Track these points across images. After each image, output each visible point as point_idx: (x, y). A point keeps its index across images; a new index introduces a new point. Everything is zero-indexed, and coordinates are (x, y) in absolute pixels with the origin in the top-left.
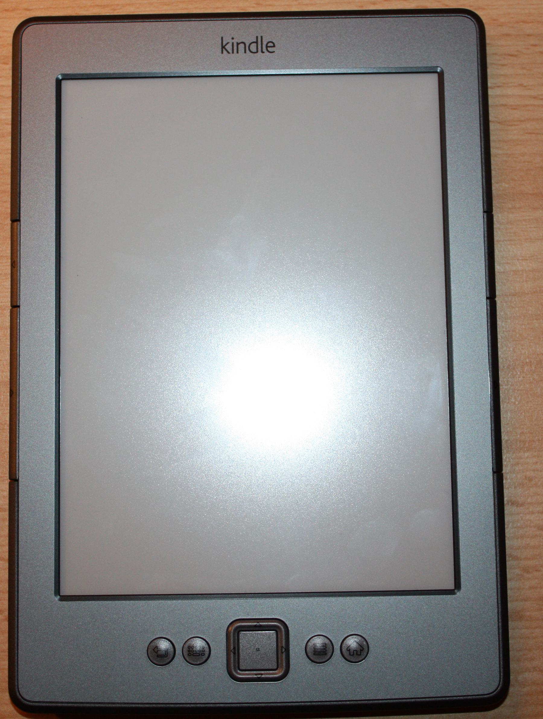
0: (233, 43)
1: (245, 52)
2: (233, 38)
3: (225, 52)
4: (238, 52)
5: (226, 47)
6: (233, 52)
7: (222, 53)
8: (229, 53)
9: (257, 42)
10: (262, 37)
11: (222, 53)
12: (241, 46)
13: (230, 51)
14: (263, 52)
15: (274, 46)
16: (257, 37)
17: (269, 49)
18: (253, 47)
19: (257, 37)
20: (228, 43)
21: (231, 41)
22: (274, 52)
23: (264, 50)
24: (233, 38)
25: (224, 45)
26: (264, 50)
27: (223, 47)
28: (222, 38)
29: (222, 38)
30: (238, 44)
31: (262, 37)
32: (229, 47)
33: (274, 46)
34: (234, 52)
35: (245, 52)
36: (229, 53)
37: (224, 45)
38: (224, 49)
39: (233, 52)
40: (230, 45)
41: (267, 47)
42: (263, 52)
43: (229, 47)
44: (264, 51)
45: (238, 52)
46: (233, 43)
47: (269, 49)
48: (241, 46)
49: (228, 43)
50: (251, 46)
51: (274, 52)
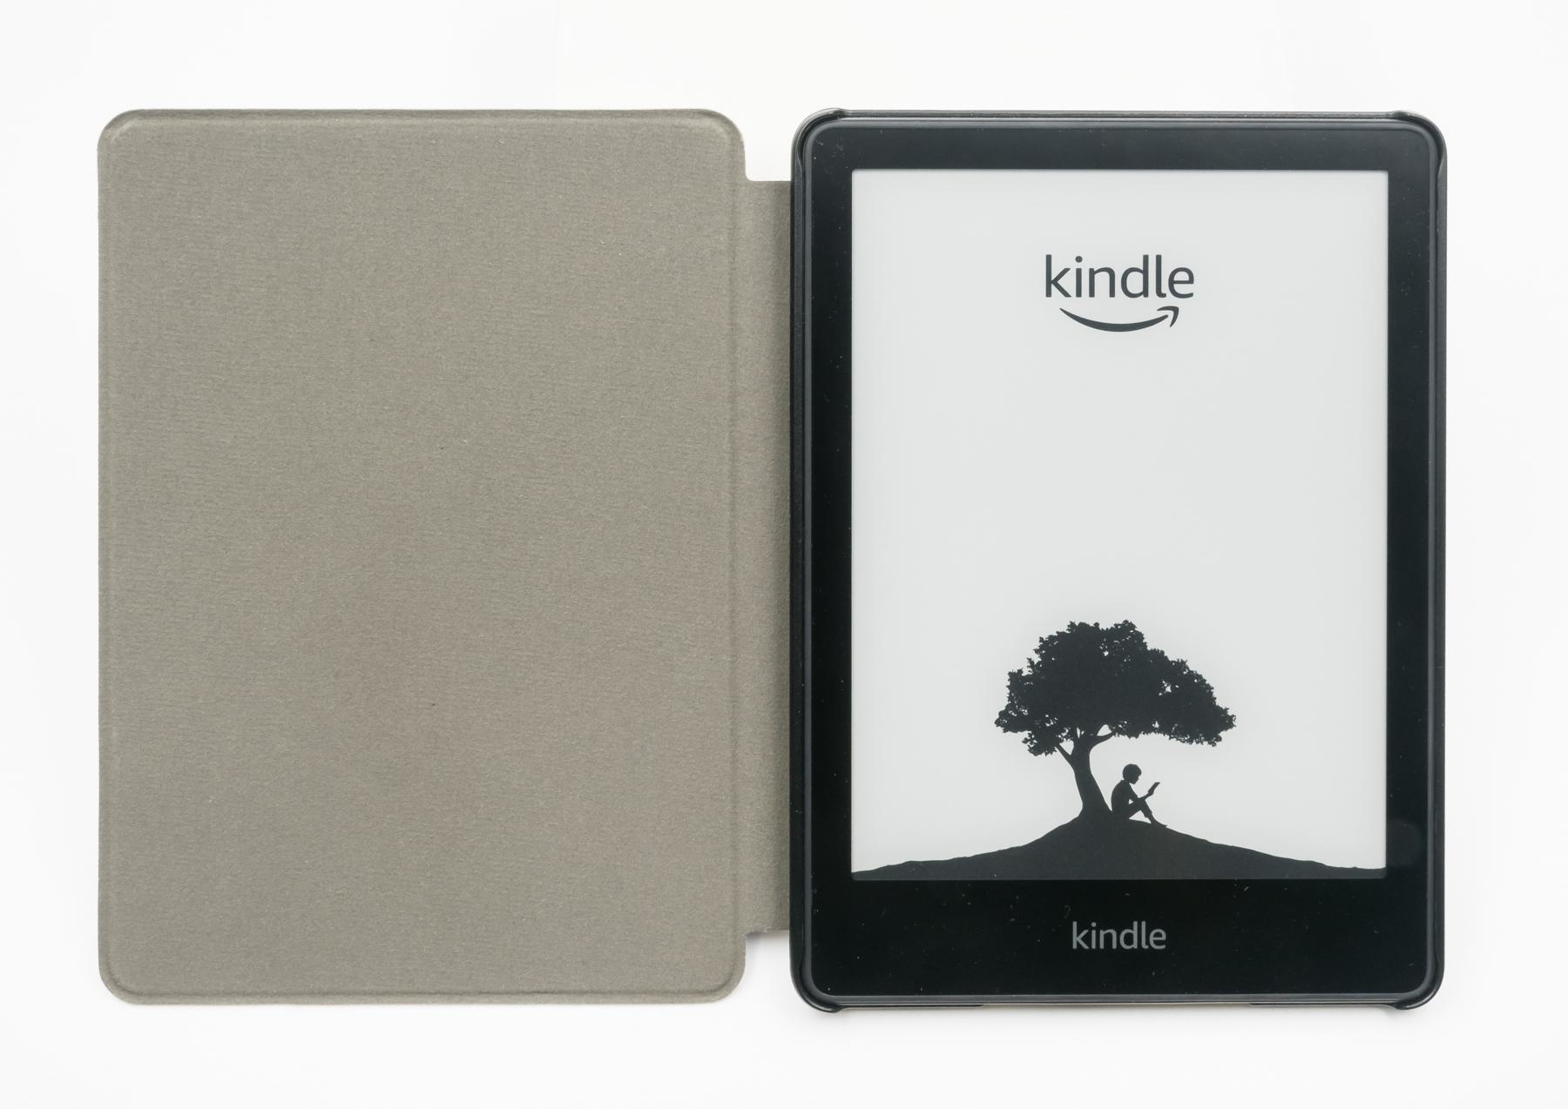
0: (1079, 272)
1: (1112, 294)
2: (1079, 259)
4: (1092, 294)
5: (1060, 282)
6: (1079, 294)
7: (1049, 294)
8: (1066, 295)
9: (1145, 272)
10: (1159, 258)
11: (1049, 294)
12: (1102, 280)
13: (1072, 290)
14: (1160, 294)
15: (1191, 281)
16: (1146, 258)
18: (1135, 283)
19: (1146, 258)
20: (1066, 271)
21: (1074, 266)
23: (1165, 288)
26: (1165, 288)
27: (1052, 283)
28: (1049, 258)
29: (1049, 258)
30: (1092, 273)
31: (1159, 258)
32: (1068, 282)
33: (1191, 281)
34: (1083, 294)
35: (1112, 294)
36: (1066, 295)
37: (1053, 277)
38: (1053, 286)
39: (1079, 294)
40: (1071, 276)
41: (1172, 282)
43: (1068, 282)
44: (1163, 291)
45: (1092, 294)
46: (1079, 272)
47: (1178, 288)
48: (1102, 280)
49: (1066, 271)
50: (1131, 276)
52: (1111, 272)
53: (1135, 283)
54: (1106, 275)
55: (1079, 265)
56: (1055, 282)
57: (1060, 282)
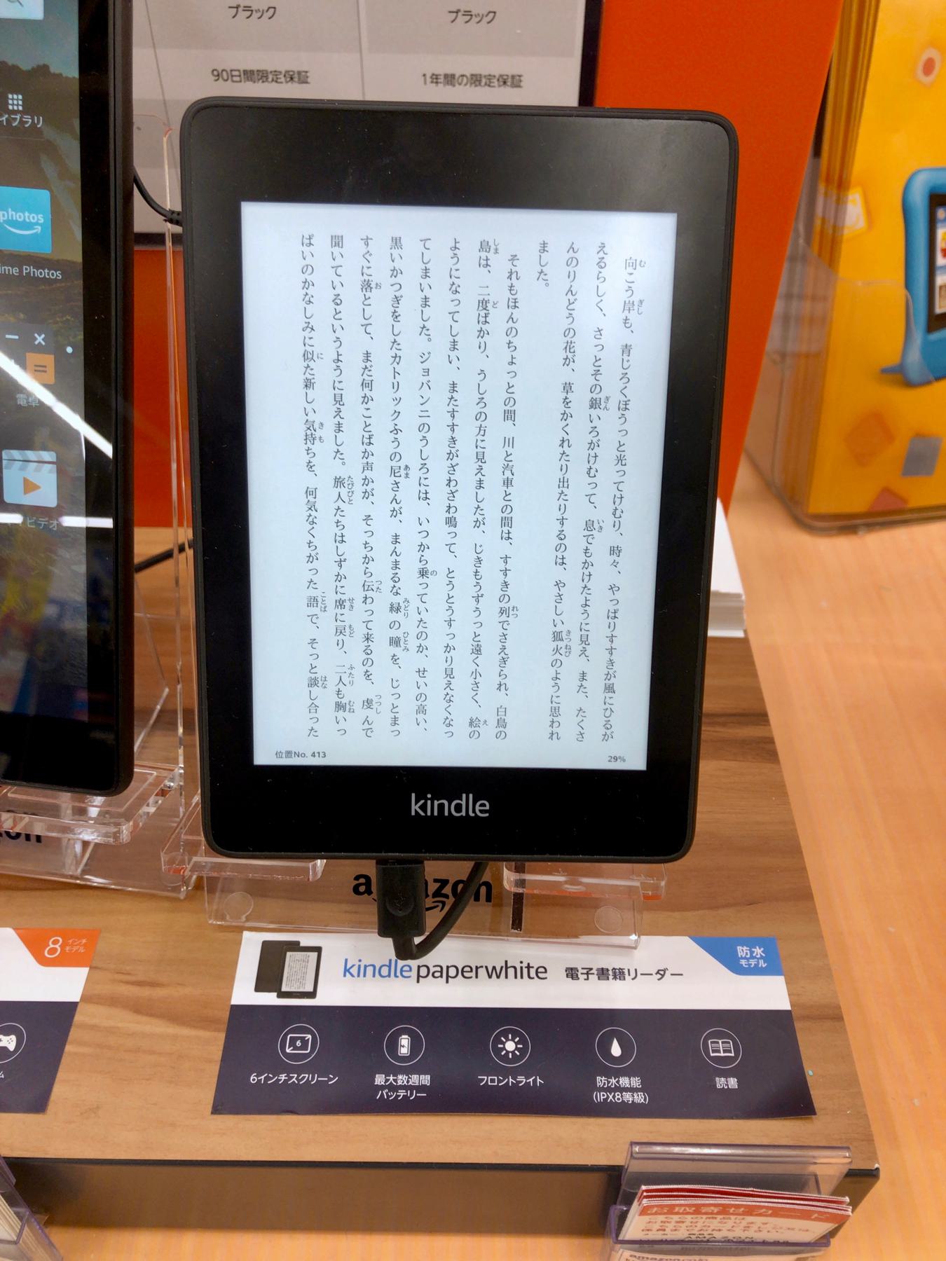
0: (359, 966)
1: (374, 976)
3: (347, 974)
4: (365, 976)
5: (351, 971)
6: (359, 976)
7: (345, 975)
8: (352, 976)
9: (390, 967)
11: (345, 975)
12: (370, 970)
13: (356, 974)
14: (396, 976)
17: (404, 974)
18: (385, 971)
20: (353, 966)
22: (409, 977)
23: (398, 974)
24: (360, 961)
25: (348, 968)
26: (398, 974)
28: (346, 960)
29: (346, 960)
30: (366, 967)
35: (374, 976)
36: (352, 976)
37: (348, 968)
38: (347, 974)
39: (359, 976)
41: (402, 971)
42: (396, 976)
43: (354, 971)
45: (365, 976)
46: (359, 966)
47: (404, 974)
48: (370, 970)
49: (353, 966)
50: (383, 968)
51: (409, 977)
52: (374, 966)
53: (385, 971)
54: (372, 968)
55: (360, 963)
56: (348, 971)
57: (351, 971)
